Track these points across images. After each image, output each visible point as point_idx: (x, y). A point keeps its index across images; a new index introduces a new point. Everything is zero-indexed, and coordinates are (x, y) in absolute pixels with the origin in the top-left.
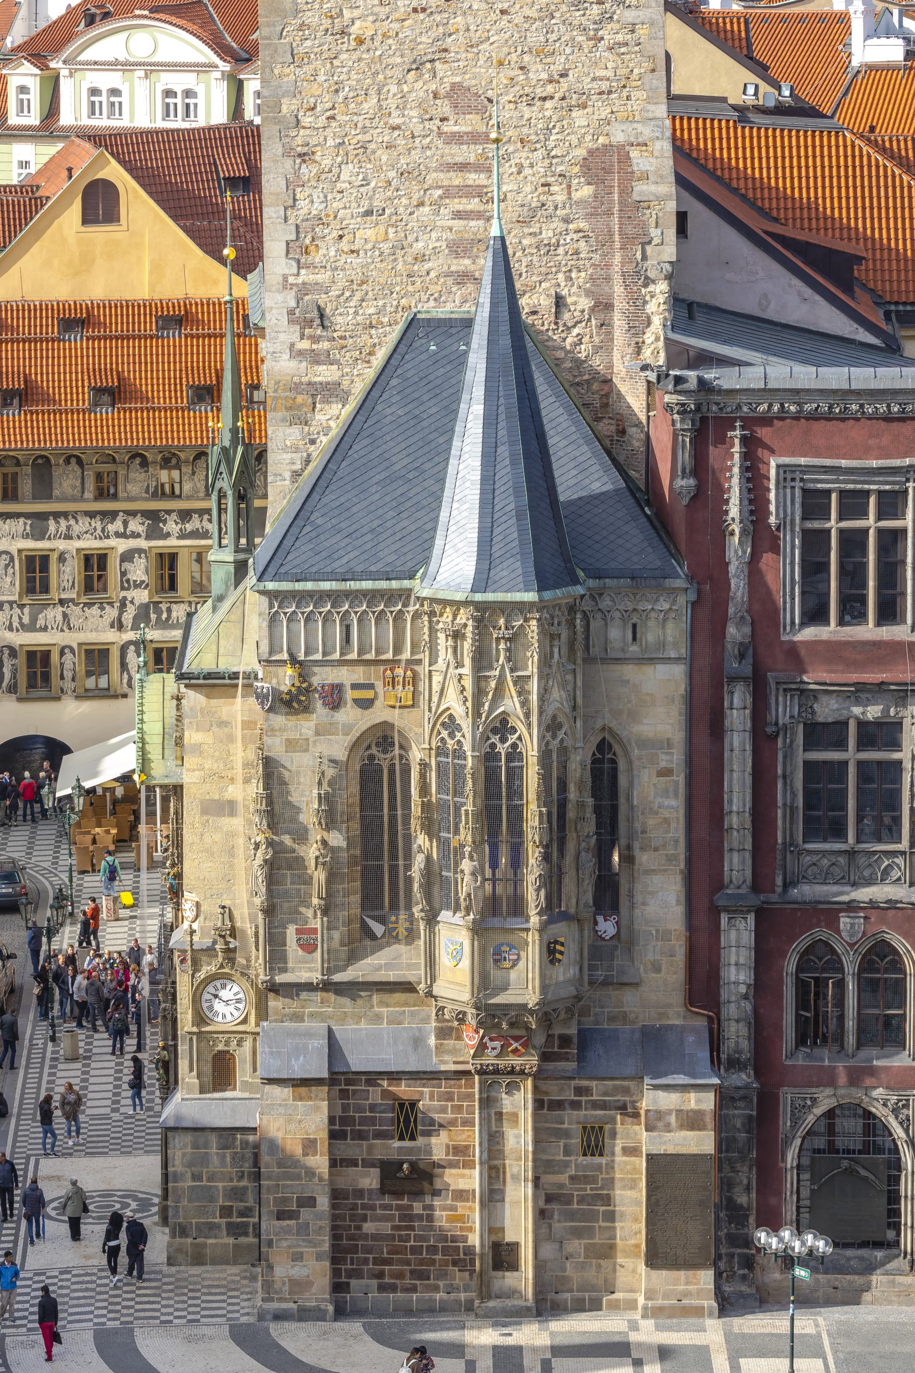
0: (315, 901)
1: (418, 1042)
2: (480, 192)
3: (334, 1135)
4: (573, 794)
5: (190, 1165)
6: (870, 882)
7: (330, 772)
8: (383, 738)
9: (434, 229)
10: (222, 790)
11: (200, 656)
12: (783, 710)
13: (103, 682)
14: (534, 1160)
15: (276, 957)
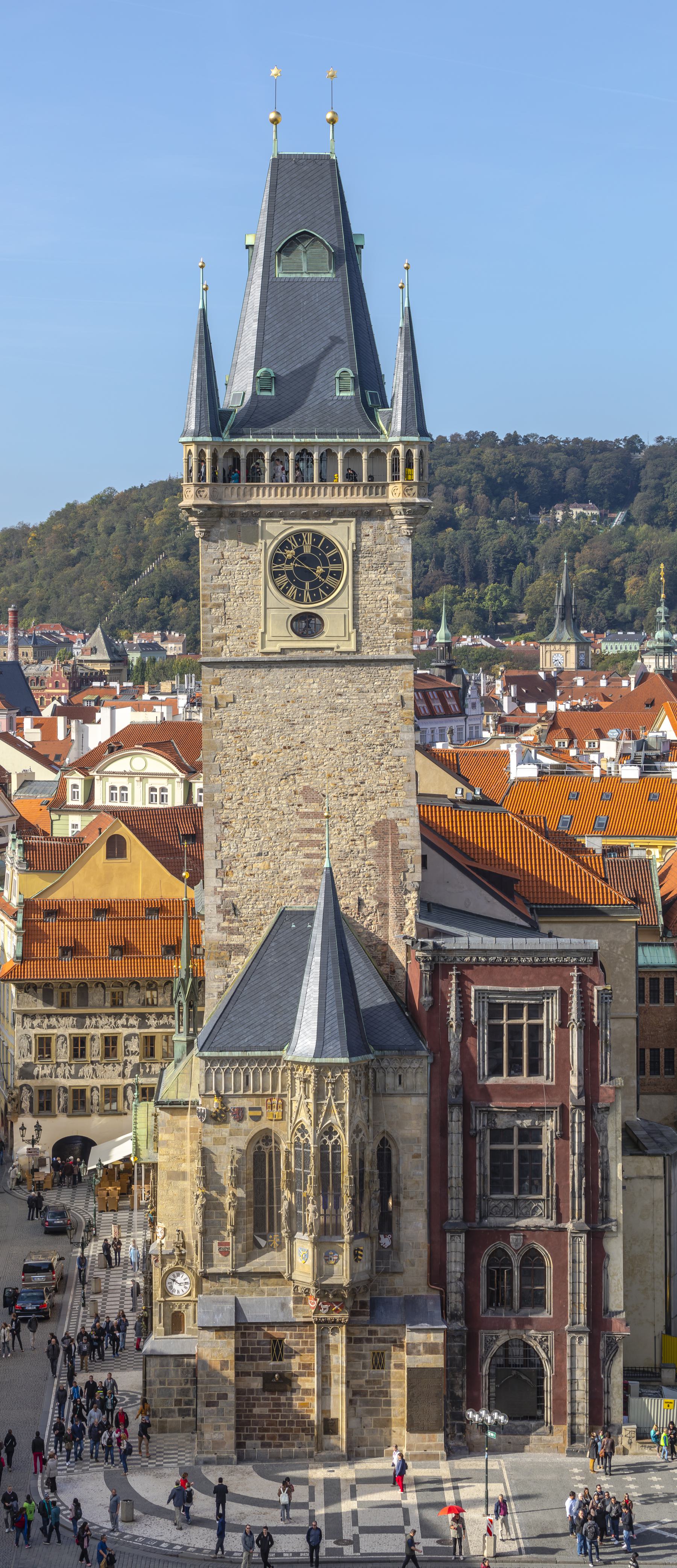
0: (229, 1227)
1: (284, 1306)
2: (319, 844)
3: (237, 1358)
4: (367, 1168)
5: (159, 1376)
6: (526, 1216)
7: (238, 1156)
8: (266, 1137)
9: (294, 864)
10: (178, 1166)
11: (167, 1093)
12: (479, 1122)
13: (114, 1106)
14: (347, 1372)
15: (208, 1259)
